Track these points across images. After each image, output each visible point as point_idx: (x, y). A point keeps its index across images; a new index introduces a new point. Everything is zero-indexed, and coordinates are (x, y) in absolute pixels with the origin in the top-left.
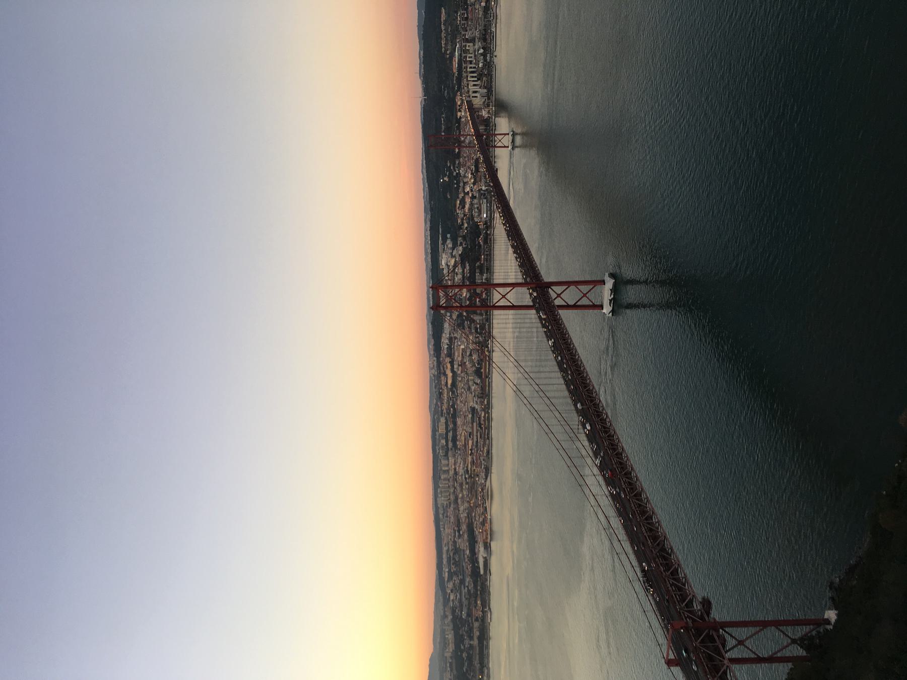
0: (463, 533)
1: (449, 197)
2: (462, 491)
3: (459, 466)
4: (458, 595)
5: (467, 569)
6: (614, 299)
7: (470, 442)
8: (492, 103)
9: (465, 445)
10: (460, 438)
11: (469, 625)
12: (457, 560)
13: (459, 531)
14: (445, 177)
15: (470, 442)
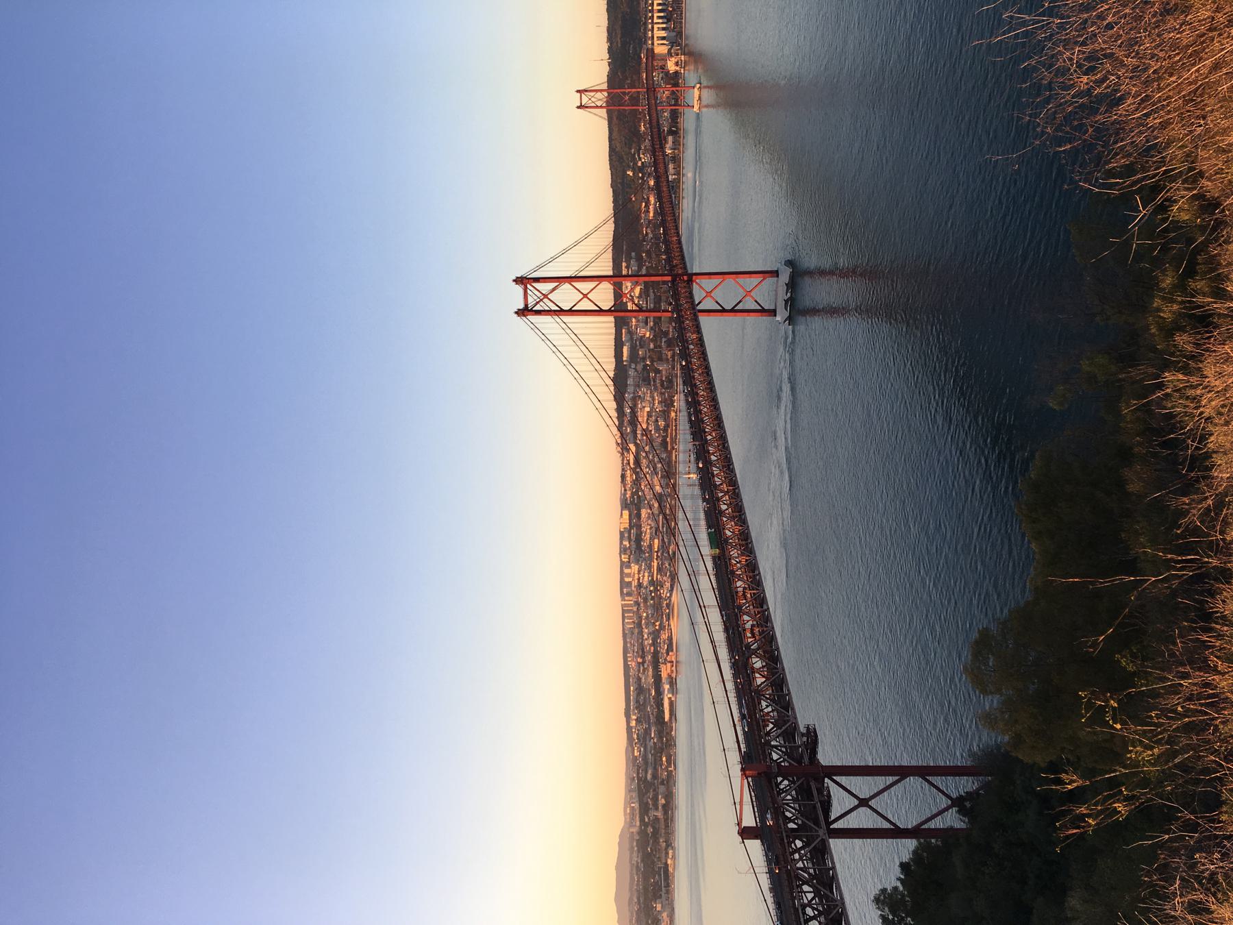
0: (648, 665)
1: (633, 199)
2: (646, 607)
3: (644, 576)
4: (642, 749)
5: (652, 714)
6: (791, 299)
7: (656, 541)
8: (681, 49)
9: (651, 546)
10: (645, 536)
11: (654, 790)
12: (641, 703)
13: (643, 663)
14: (629, 170)
15: (656, 541)
